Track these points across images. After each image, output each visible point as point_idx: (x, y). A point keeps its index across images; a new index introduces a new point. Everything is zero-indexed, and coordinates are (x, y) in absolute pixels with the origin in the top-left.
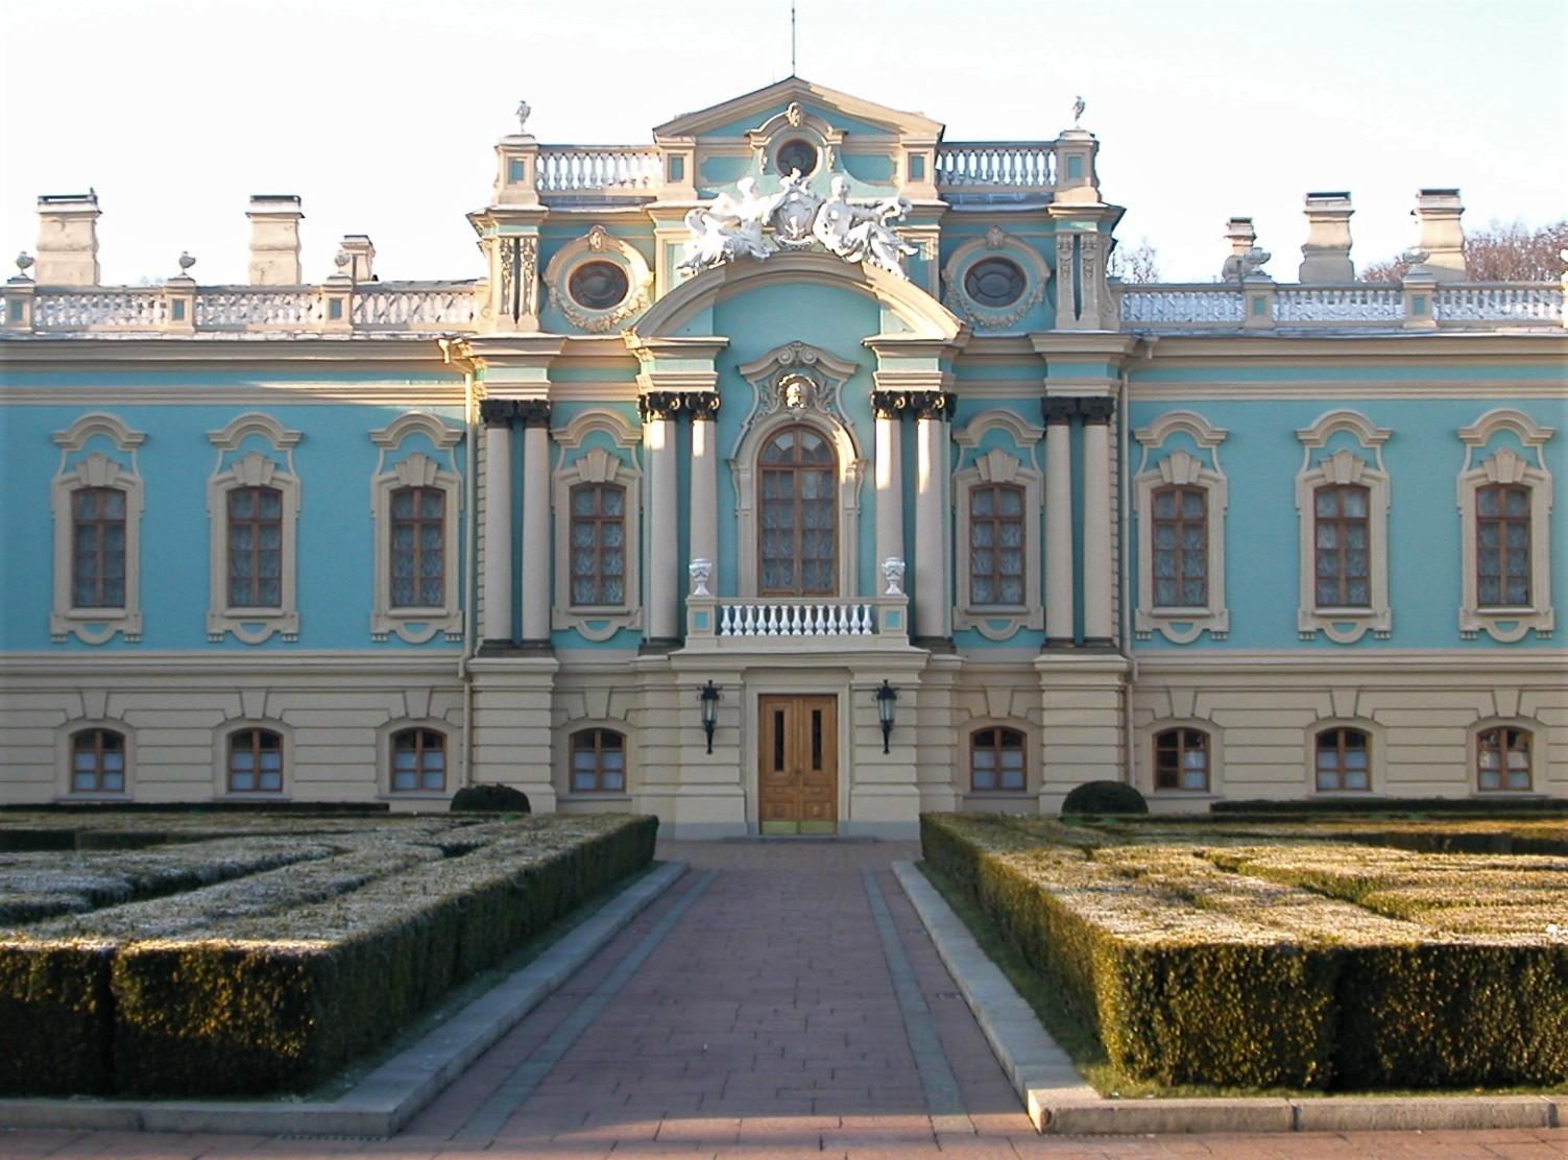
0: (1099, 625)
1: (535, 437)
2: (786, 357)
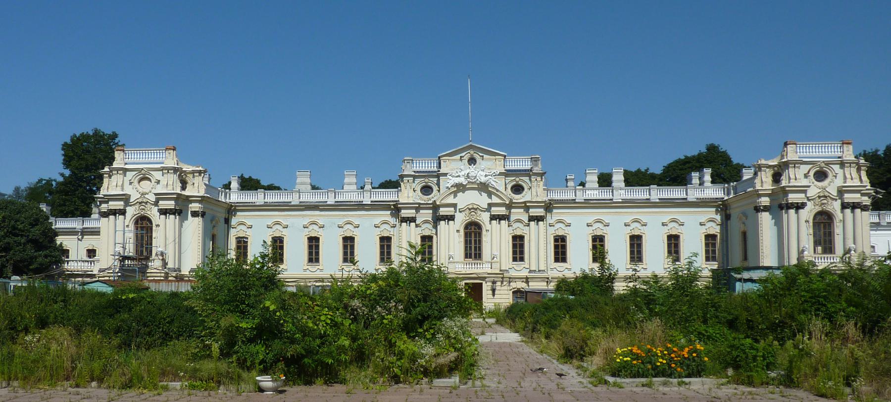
1: (413, 224)
2: (470, 207)
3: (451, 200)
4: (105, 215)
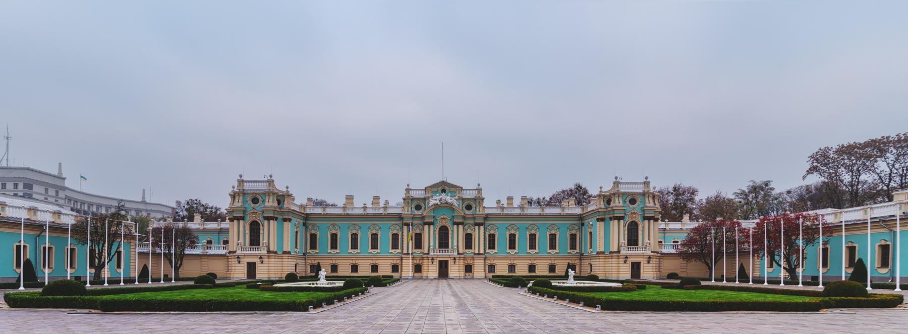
0: (482, 251)
3: (432, 214)
4: (232, 220)
